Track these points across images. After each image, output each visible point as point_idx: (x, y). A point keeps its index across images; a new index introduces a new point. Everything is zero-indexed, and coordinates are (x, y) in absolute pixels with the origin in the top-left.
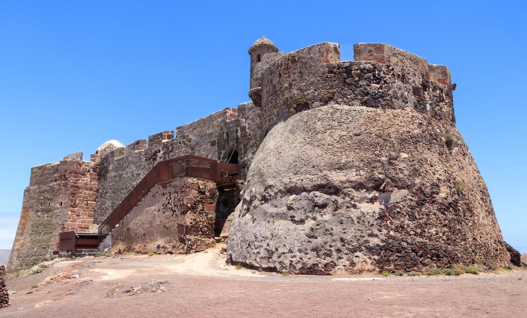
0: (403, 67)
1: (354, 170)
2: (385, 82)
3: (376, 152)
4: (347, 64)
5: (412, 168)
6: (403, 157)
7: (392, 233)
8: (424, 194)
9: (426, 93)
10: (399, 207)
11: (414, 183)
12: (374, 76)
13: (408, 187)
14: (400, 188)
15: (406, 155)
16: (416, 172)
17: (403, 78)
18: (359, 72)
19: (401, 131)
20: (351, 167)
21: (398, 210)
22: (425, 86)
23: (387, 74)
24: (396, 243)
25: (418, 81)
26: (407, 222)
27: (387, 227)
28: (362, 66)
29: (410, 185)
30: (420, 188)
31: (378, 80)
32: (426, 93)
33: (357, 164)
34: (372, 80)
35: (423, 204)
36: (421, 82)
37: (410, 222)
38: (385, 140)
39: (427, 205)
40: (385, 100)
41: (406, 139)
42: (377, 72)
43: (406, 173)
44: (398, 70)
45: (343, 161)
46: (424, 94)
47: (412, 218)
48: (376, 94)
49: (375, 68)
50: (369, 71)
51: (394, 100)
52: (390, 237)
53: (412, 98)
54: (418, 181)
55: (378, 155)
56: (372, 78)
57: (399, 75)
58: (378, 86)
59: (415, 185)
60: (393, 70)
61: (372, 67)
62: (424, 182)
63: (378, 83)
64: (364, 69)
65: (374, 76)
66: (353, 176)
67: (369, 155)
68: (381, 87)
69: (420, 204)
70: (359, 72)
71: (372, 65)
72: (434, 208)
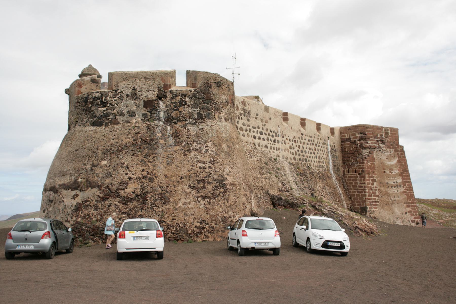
0: (134, 87)
1: (69, 176)
2: (111, 104)
3: (86, 162)
4: (86, 96)
5: (106, 172)
6: (102, 164)
7: (79, 220)
8: (111, 191)
9: (161, 103)
10: (89, 201)
11: (104, 184)
12: (101, 101)
13: (99, 187)
14: (92, 187)
15: (105, 162)
16: (110, 175)
17: (134, 95)
18: (92, 100)
19: (109, 144)
20: (68, 174)
21: (88, 203)
22: (160, 97)
23: (114, 98)
24: (79, 227)
25: (152, 95)
26: (92, 211)
27: (77, 216)
28: (94, 95)
29: (100, 185)
30: (108, 186)
31: (104, 104)
32: (161, 103)
33: (71, 172)
34: (99, 105)
35: (107, 199)
36: (156, 95)
37: (95, 212)
38: (94, 152)
39: (110, 199)
40: (109, 119)
41: (111, 149)
42: (104, 98)
43: (101, 176)
44: (129, 91)
45: (65, 170)
46: (158, 104)
47: (96, 208)
48: (101, 116)
49: (102, 95)
50: (98, 98)
51: (117, 117)
52: (77, 222)
53: (144, 111)
54: (107, 181)
55: (85, 165)
56: (100, 103)
57: (128, 96)
58: (104, 109)
59: (104, 184)
60: (121, 92)
61: (100, 95)
62: (113, 182)
63: (105, 106)
64: (95, 97)
65: (101, 101)
66: (67, 180)
67: (80, 165)
68: (107, 110)
69: (104, 199)
70: (92, 100)
71: (100, 93)
72: (116, 201)
